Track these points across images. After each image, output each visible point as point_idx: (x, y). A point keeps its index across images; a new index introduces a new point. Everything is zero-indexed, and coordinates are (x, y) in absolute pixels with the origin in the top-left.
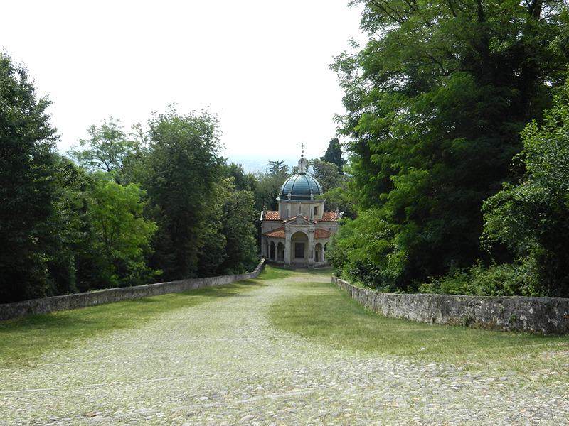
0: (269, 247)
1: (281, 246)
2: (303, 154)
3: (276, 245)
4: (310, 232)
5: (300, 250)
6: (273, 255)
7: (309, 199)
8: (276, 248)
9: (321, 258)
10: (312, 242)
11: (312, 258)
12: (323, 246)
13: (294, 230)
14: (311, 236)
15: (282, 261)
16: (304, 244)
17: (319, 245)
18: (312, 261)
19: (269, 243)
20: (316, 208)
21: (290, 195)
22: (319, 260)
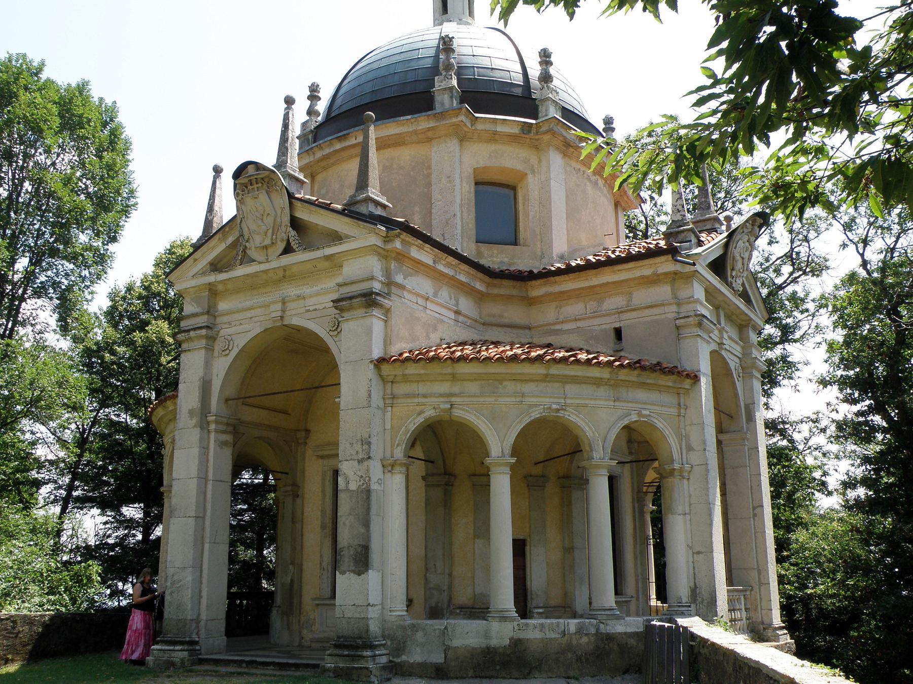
12: (499, 444)
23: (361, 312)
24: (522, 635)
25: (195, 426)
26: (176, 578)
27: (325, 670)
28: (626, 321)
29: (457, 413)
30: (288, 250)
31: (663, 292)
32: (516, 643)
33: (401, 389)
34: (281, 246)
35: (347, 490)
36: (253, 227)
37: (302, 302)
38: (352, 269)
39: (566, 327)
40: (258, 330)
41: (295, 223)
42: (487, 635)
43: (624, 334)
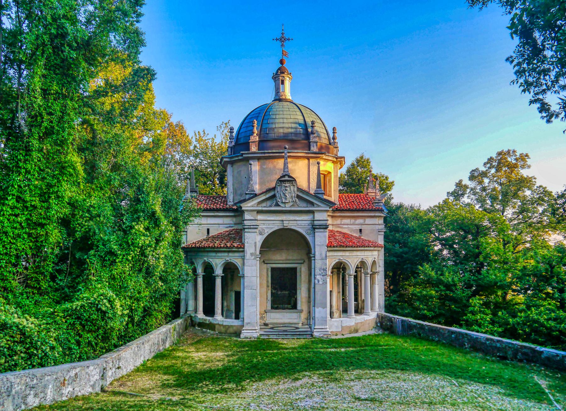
1: (232, 273)
2: (285, 58)
3: (219, 271)
8: (218, 282)
13: (270, 224)
14: (320, 240)
15: (237, 317)
16: (296, 268)
17: (340, 269)
23: (322, 230)
28: (363, 227)
34: (291, 204)
37: (295, 222)
38: (318, 216)
39: (344, 226)
40: (276, 228)
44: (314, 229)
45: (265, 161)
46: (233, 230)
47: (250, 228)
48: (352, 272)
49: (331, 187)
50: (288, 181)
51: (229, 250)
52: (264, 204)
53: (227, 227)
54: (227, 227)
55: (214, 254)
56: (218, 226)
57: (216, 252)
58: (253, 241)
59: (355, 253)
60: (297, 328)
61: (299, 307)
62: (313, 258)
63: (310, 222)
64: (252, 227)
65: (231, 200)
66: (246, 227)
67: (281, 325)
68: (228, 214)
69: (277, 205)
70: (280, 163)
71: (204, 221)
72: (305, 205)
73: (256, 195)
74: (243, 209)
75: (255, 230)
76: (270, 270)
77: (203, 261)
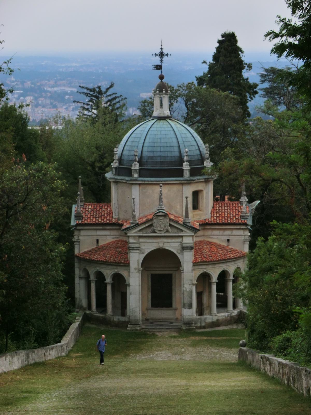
0: (93, 286)
3: (109, 280)
4: (184, 248)
5: (162, 289)
6: (101, 304)
7: (180, 173)
8: (109, 288)
9: (210, 307)
10: (189, 274)
11: (190, 306)
13: (149, 246)
14: (187, 259)
15: (124, 313)
18: (190, 313)
19: (92, 277)
20: (196, 194)
21: (136, 166)
22: (206, 312)
24: (218, 318)
25: (137, 272)
26: (133, 309)
27: (183, 329)
28: (230, 238)
29: (207, 272)
30: (167, 231)
31: (241, 232)
32: (218, 320)
33: (196, 267)
35: (186, 291)
36: (158, 226)
37: (169, 244)
39: (214, 237)
40: (154, 248)
41: (170, 225)
42: (213, 319)
43: (230, 241)
44: (183, 249)
45: (145, 186)
46: (119, 241)
47: (134, 249)
48: (215, 279)
49: (203, 203)
50: (162, 215)
51: (118, 264)
52: (144, 231)
53: (113, 238)
54: (113, 238)
55: (105, 266)
56: (106, 237)
57: (108, 265)
58: (136, 259)
59: (217, 265)
60: (172, 323)
61: (174, 306)
62: (182, 271)
63: (179, 244)
64: (135, 248)
65: (117, 214)
66: (130, 248)
67: (159, 320)
68: (114, 228)
69: (154, 232)
70: (157, 189)
71: (93, 233)
72: (175, 230)
73: (138, 225)
74: (128, 235)
75: (138, 251)
76: (150, 276)
77: (96, 270)
